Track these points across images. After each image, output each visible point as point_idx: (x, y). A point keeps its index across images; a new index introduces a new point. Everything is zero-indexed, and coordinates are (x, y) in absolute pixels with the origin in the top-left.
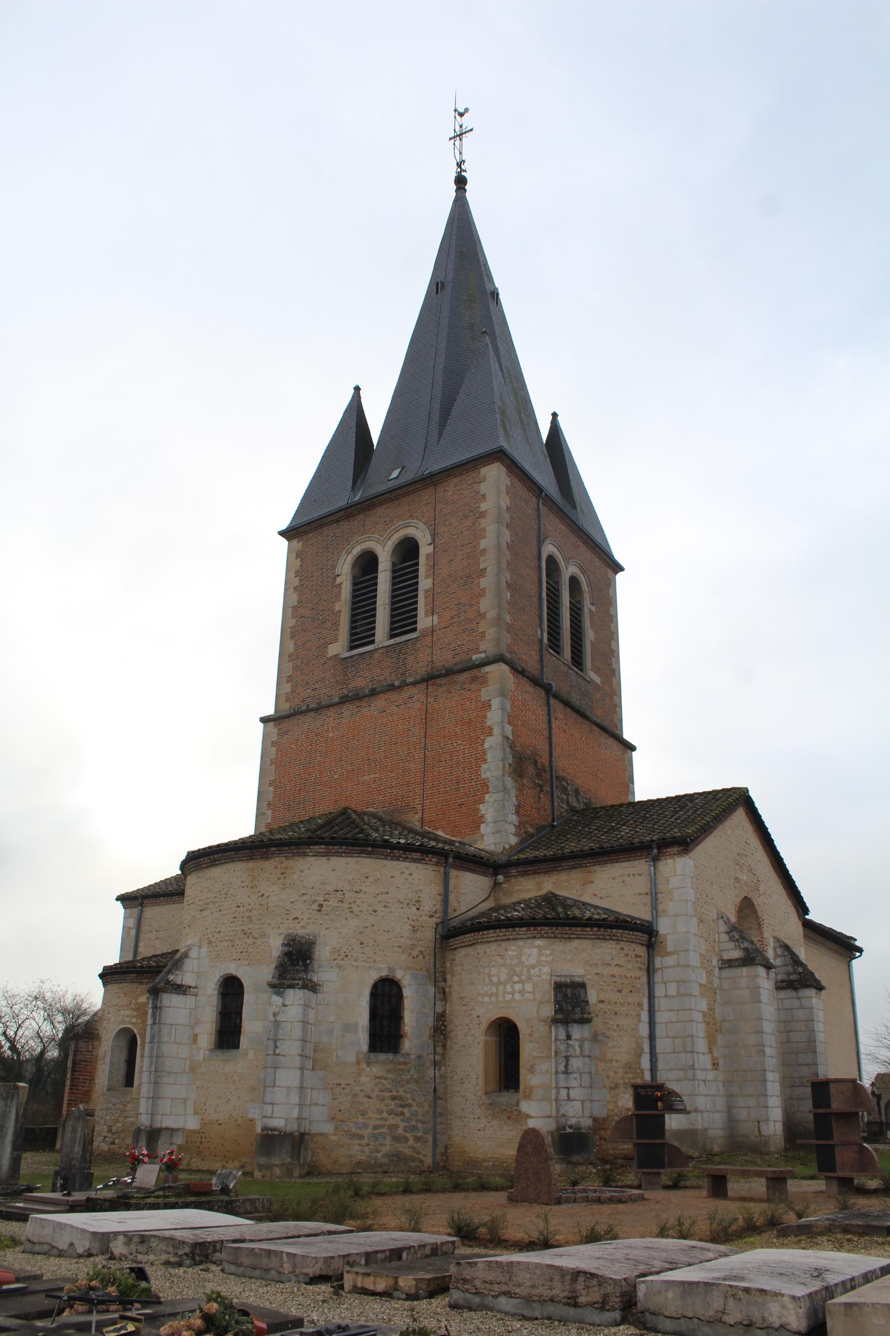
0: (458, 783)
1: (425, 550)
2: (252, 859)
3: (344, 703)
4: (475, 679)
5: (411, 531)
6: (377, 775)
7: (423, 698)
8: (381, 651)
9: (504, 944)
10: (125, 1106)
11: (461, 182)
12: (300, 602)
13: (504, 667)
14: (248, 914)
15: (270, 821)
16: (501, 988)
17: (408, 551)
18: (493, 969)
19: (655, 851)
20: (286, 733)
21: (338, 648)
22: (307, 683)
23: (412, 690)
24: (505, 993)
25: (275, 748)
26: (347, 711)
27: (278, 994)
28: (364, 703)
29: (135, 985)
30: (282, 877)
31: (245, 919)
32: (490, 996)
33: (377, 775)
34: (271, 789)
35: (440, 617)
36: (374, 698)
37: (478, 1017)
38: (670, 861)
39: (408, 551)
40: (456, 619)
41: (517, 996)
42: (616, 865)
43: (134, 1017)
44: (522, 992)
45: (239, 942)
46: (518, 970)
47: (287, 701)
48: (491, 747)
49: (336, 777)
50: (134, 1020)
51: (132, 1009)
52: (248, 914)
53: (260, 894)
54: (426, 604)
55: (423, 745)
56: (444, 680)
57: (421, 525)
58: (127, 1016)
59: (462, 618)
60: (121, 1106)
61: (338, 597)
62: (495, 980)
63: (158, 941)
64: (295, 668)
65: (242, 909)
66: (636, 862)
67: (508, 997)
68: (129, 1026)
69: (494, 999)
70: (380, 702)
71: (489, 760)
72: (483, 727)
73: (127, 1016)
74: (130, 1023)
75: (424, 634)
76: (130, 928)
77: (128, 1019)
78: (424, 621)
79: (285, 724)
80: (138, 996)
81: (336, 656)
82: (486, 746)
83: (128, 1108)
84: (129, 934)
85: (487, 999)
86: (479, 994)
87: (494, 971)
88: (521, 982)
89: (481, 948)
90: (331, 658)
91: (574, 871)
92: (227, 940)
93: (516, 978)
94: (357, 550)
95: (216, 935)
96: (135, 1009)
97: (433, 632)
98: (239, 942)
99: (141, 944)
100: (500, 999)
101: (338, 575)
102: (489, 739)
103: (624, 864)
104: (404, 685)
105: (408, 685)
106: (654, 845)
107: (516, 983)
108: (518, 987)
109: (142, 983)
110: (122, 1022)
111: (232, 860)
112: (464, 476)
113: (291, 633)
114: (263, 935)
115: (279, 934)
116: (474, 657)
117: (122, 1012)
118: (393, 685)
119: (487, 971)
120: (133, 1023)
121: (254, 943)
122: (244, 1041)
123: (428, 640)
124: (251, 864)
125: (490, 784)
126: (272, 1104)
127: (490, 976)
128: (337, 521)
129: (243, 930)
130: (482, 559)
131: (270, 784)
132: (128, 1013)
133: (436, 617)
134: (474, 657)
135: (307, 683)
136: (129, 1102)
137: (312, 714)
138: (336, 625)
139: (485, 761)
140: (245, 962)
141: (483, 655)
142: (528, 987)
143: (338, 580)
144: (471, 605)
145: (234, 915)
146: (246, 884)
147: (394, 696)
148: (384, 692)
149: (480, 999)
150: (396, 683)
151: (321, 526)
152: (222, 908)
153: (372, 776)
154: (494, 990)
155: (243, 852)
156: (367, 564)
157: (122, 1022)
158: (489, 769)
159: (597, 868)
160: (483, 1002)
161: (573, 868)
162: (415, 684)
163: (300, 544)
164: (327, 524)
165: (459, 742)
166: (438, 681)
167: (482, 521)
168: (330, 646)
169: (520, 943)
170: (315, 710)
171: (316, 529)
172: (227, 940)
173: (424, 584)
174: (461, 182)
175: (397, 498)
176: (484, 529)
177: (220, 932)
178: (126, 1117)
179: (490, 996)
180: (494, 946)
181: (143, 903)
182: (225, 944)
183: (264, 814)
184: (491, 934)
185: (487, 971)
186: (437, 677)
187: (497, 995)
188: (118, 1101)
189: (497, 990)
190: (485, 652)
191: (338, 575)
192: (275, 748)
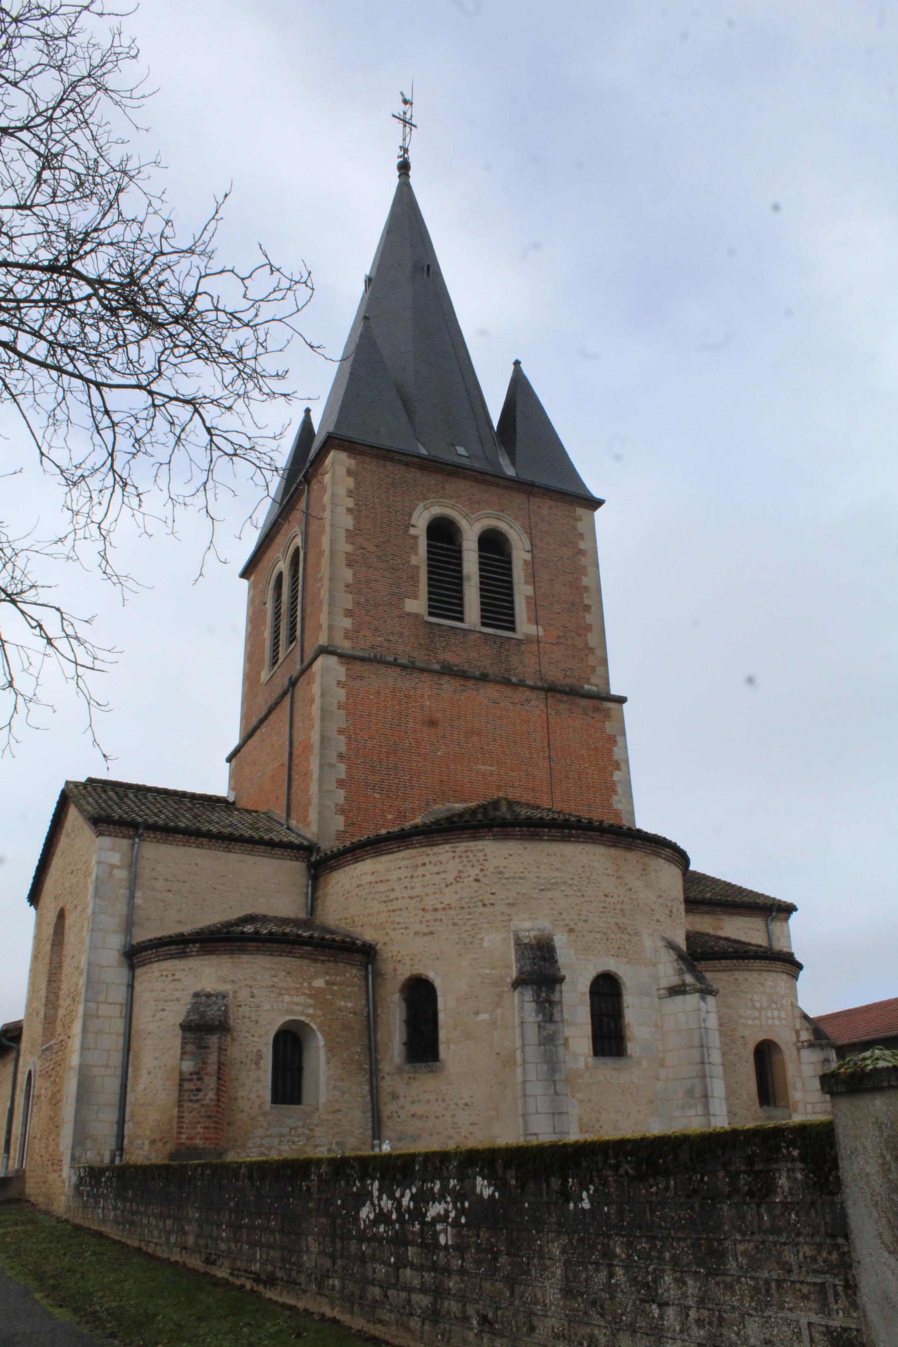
0: (590, 806)
1: (520, 554)
2: (613, 846)
3: (443, 674)
4: (597, 710)
5: (503, 526)
6: (494, 769)
7: (542, 706)
8: (478, 635)
9: (764, 974)
10: (312, 1130)
11: (404, 167)
12: (357, 528)
13: (333, 660)
14: (619, 906)
15: (343, 776)
16: (763, 1012)
17: (493, 544)
18: (755, 995)
19: (774, 914)
20: (361, 678)
21: (418, 605)
22: (376, 629)
23: (528, 693)
24: (768, 1018)
25: (343, 691)
26: (448, 685)
27: (704, 999)
28: (470, 683)
29: (305, 962)
30: (644, 872)
31: (617, 911)
32: (754, 1020)
33: (494, 769)
34: (343, 738)
35: (545, 630)
36: (482, 683)
37: (743, 1037)
38: (778, 924)
39: (493, 544)
40: (563, 641)
41: (777, 1022)
42: (740, 918)
43: (310, 1006)
44: (779, 1018)
45: (613, 936)
46: (775, 998)
47: (347, 637)
48: (620, 781)
49: (439, 753)
50: (311, 1011)
51: (304, 994)
52: (619, 906)
53: (628, 887)
54: (528, 611)
55: (547, 754)
56: (565, 698)
57: (517, 526)
58: (297, 1004)
59: (570, 642)
60: (307, 1131)
61: (414, 548)
62: (758, 1005)
63: (170, 895)
64: (357, 603)
65: (609, 899)
66: (755, 919)
67: (770, 1022)
68: (302, 1018)
69: (757, 1022)
70: (491, 691)
71: (620, 792)
72: (610, 759)
73: (297, 1004)
74: (302, 1014)
75: (528, 639)
76: (113, 867)
77: (299, 1008)
78: (524, 626)
79: (358, 667)
80: (311, 978)
81: (417, 615)
82: (615, 778)
83: (317, 1134)
84: (111, 875)
85: (750, 1022)
86: (741, 1017)
87: (756, 997)
88: (777, 1009)
89: (740, 976)
90: (409, 614)
91: (708, 916)
92: (599, 932)
93: (774, 1006)
94: (436, 511)
95: (581, 924)
96: (311, 996)
97: (539, 642)
98: (613, 936)
99: (138, 894)
100: (764, 1023)
101: (413, 526)
102: (617, 773)
103: (746, 919)
104: (521, 684)
105: (525, 686)
106: (775, 909)
107: (774, 1009)
108: (776, 1013)
109: (316, 961)
110: (289, 1012)
111: (594, 841)
112: (559, 504)
113: (347, 559)
114: (637, 933)
115: (650, 935)
116: (586, 687)
117: (287, 998)
118: (509, 680)
119: (749, 996)
120: (308, 1015)
121: (630, 941)
122: (632, 1047)
123: (534, 648)
124: (613, 851)
125: (622, 816)
126: (714, 1115)
127: (752, 1000)
128: (407, 464)
129: (617, 924)
130: (585, 595)
131: (341, 732)
132: (301, 999)
133: (540, 628)
134: (586, 687)
135: (376, 629)
136: (317, 1125)
137: (398, 669)
138: (414, 579)
139: (615, 792)
140: (624, 959)
141: (595, 688)
142: (783, 1014)
143: (412, 531)
144: (580, 635)
145: (603, 905)
146: (610, 872)
147: (508, 691)
148: (497, 682)
149: (743, 1021)
150: (514, 680)
151: (385, 458)
152: (584, 893)
153: (488, 768)
154: (757, 1014)
155: (609, 835)
156: (443, 533)
157: (289, 1012)
158: (620, 802)
159: (725, 917)
160: (746, 1024)
161: (707, 913)
162: (533, 688)
163: (353, 462)
164: (392, 460)
165: (587, 765)
166: (558, 695)
167: (583, 559)
168: (407, 600)
169: (774, 975)
170: (404, 667)
171: (377, 457)
172: (599, 932)
173: (522, 590)
174: (404, 167)
175: (484, 482)
176: (585, 567)
177: (586, 921)
178: (316, 1146)
179: (754, 1020)
180: (755, 975)
181: (142, 835)
182: (599, 936)
183: (333, 766)
184: (757, 963)
185: (749, 996)
186: (559, 691)
187: (760, 1018)
188: (300, 1123)
189: (760, 1014)
190: (597, 686)
191: (413, 526)
192: (343, 691)
